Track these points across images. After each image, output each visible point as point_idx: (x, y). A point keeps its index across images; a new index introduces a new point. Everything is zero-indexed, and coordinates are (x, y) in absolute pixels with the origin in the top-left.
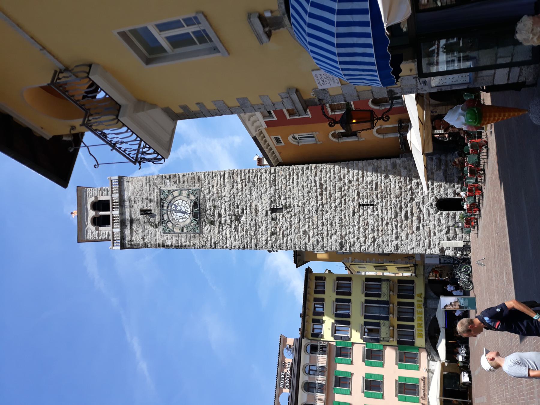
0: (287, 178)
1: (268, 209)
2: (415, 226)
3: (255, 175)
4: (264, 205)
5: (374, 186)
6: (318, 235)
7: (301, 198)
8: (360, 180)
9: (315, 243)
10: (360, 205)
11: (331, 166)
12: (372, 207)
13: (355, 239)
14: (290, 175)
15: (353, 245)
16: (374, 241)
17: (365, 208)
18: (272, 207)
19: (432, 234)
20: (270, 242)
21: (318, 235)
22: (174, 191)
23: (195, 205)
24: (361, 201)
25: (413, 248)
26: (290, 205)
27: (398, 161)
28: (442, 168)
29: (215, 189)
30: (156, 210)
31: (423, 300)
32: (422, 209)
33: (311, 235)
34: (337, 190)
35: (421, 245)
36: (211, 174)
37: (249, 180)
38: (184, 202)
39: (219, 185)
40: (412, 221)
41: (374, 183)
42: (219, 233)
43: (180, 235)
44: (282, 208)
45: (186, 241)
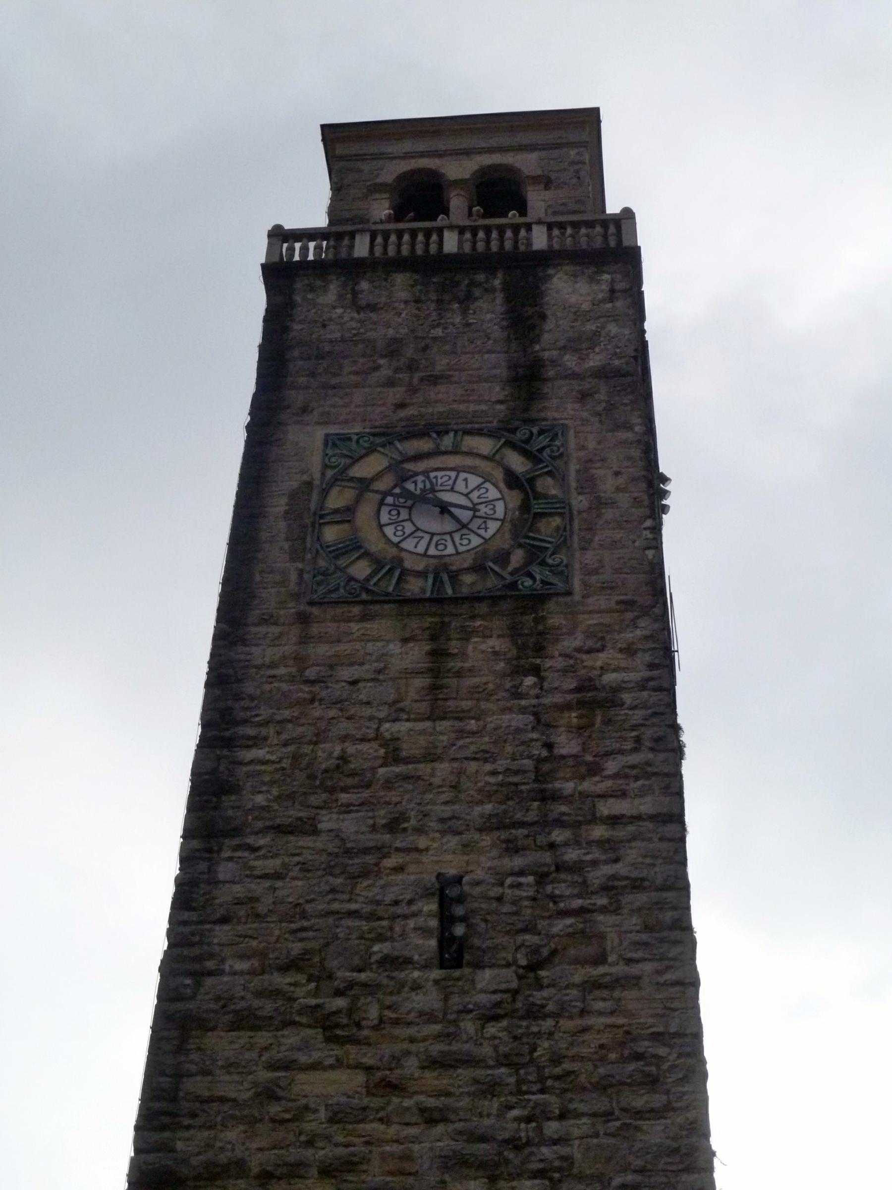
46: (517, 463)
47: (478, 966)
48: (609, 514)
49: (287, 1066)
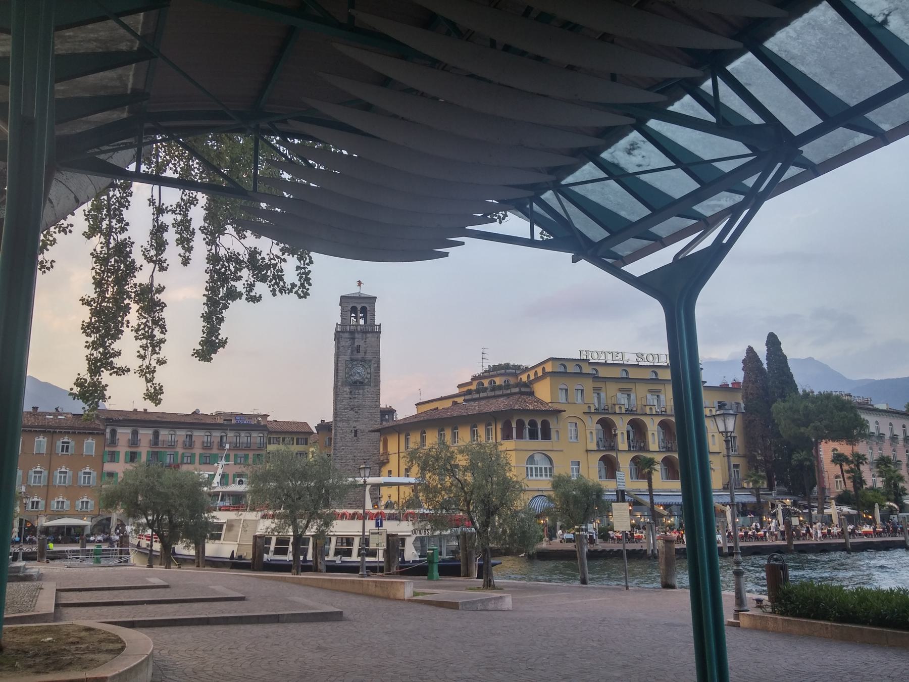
4: (359, 426)
23: (361, 383)
30: (360, 356)
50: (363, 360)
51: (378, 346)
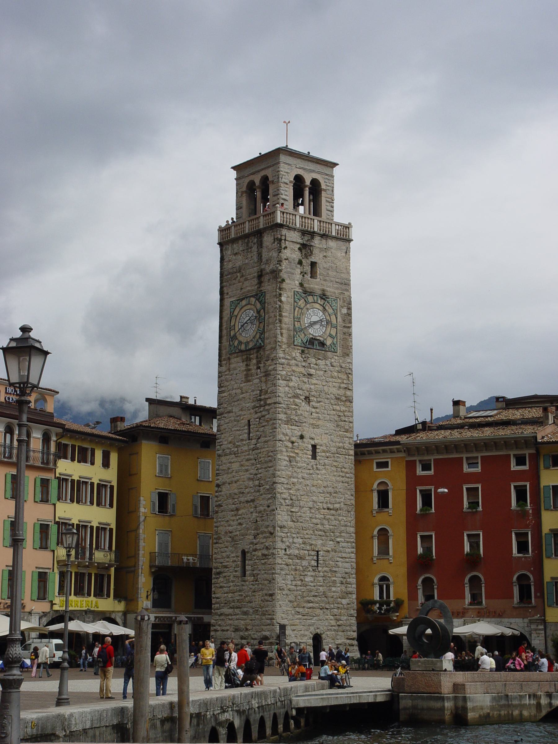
0: (343, 469)
1: (316, 441)
2: (301, 610)
3: (348, 430)
5: (334, 569)
6: (292, 500)
7: (325, 484)
8: (340, 555)
9: (284, 496)
10: (318, 552)
11: (353, 522)
12: (316, 565)
13: (288, 543)
14: (347, 473)
15: (282, 541)
16: (287, 565)
17: (315, 558)
18: (318, 447)
19: (294, 627)
20: (284, 439)
21: (292, 500)
22: (337, 318)
24: (321, 553)
25: (281, 607)
26: (319, 470)
27: (354, 596)
28: (348, 641)
29: (336, 374)
31: (92, 609)
32: (315, 618)
33: (291, 491)
34: (331, 527)
35: (283, 615)
36: (350, 372)
37: (344, 421)
38: (325, 328)
39: (340, 381)
40: (304, 607)
41: (337, 569)
42: (294, 371)
43: (292, 316)
44: (315, 459)
45: (285, 324)
46: (259, 306)
47: (252, 439)
48: (271, 320)
49: (230, 463)
50: (324, 296)
51: (349, 273)
